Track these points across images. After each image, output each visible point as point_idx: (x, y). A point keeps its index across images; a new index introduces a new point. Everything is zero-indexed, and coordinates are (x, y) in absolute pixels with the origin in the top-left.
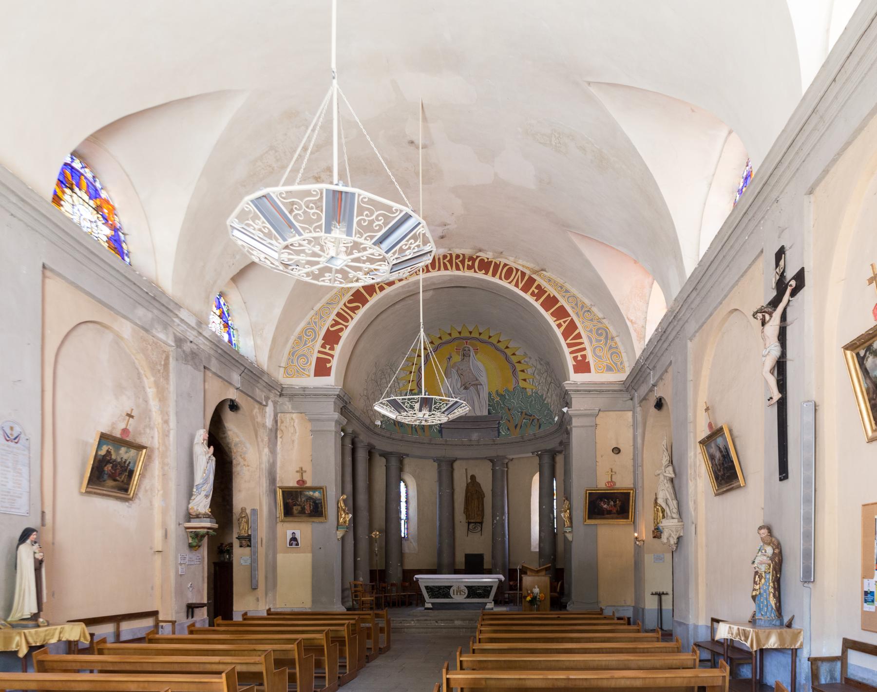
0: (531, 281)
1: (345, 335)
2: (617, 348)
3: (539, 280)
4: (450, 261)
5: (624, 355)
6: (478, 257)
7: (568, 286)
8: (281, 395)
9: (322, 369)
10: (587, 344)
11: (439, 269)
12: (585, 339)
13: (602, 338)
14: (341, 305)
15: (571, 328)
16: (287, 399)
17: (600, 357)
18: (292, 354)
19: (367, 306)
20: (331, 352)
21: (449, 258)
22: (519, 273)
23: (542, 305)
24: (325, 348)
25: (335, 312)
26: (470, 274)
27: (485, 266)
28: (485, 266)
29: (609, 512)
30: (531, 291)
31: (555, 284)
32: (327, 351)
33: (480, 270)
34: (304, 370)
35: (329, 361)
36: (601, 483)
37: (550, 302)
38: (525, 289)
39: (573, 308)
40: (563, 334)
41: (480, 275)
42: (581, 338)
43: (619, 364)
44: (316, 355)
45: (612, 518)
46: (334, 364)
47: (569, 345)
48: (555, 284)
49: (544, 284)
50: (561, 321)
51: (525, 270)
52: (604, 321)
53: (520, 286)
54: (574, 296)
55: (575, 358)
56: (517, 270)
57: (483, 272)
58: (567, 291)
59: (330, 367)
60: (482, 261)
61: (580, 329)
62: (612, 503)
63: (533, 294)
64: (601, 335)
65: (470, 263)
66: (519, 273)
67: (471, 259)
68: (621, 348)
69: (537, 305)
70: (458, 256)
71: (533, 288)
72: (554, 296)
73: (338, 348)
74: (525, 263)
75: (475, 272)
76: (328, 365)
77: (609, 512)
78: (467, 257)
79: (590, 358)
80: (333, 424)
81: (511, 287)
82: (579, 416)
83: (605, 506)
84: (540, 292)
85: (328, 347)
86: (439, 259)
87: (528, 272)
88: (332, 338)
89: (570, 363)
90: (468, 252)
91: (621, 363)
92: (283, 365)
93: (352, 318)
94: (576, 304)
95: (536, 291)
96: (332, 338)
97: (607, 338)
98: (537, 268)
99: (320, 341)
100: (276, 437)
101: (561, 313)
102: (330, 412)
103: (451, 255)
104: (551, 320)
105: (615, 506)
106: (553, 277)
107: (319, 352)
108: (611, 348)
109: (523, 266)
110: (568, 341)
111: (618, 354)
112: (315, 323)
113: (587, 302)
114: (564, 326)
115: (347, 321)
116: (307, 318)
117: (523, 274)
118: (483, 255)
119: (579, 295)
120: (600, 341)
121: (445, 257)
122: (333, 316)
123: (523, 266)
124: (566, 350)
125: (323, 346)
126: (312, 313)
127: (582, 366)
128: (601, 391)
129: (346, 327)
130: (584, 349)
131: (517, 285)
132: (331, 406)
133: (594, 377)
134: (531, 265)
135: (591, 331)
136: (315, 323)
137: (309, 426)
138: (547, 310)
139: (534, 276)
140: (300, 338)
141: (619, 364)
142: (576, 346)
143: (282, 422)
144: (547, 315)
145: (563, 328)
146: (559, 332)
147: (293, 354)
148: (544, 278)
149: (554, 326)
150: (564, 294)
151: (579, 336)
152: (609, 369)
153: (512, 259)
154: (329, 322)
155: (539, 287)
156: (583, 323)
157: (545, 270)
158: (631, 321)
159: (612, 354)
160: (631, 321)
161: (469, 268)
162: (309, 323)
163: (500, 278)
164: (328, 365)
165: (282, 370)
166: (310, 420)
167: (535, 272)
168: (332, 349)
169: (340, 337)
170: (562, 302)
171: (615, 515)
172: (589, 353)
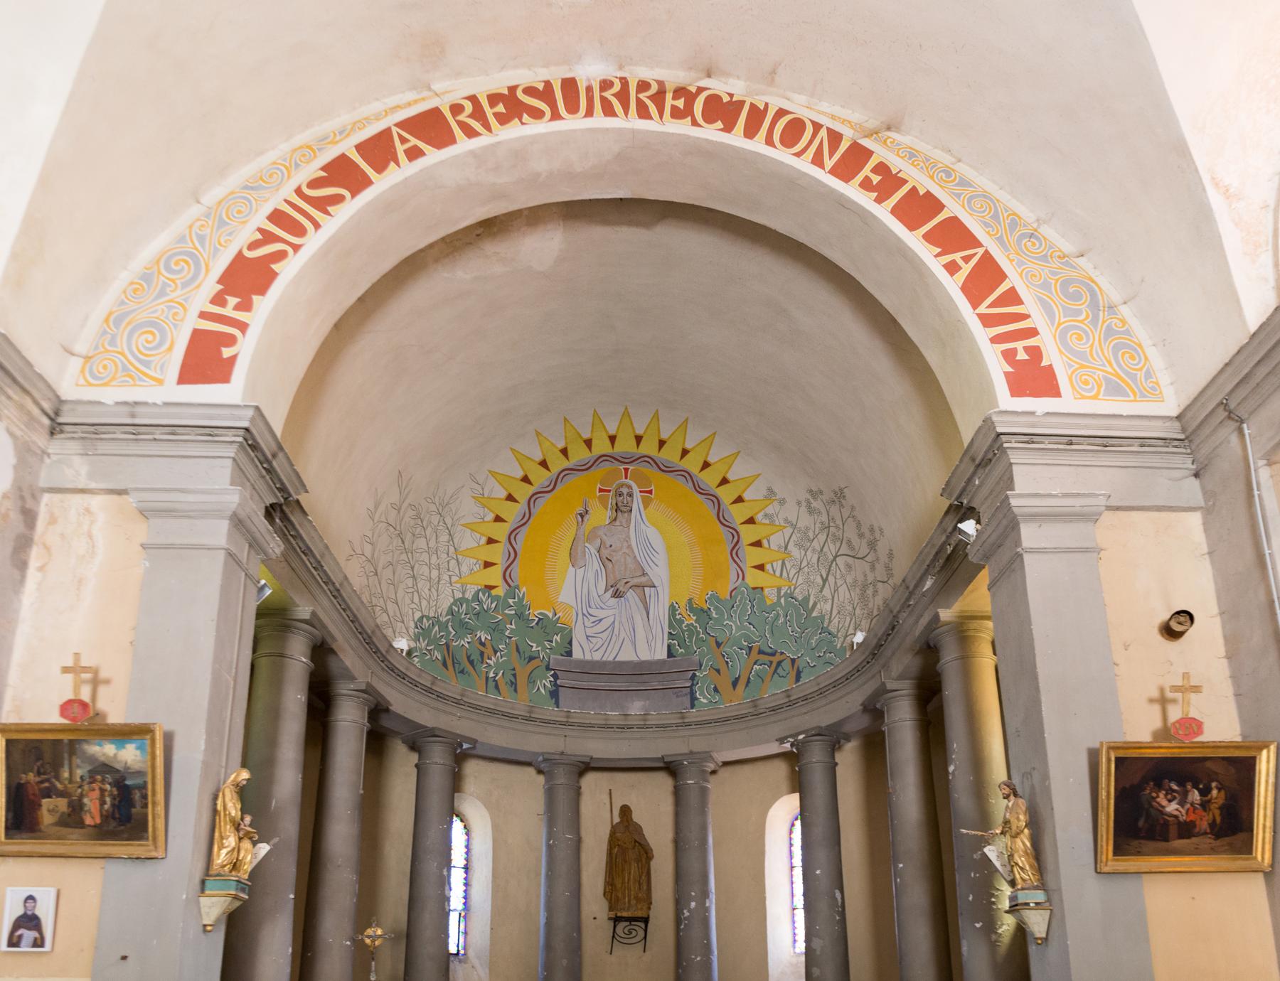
0: (858, 155)
1: (287, 271)
2: (1127, 332)
3: (881, 153)
4: (623, 96)
5: (1151, 352)
6: (701, 90)
7: (964, 169)
8: (55, 429)
9: (206, 360)
10: (1038, 319)
11: (589, 113)
12: (1030, 304)
13: (1085, 312)
14: (288, 191)
15: (985, 278)
16: (74, 446)
17: (1080, 355)
18: (115, 319)
19: (367, 195)
20: (241, 316)
21: (617, 87)
22: (823, 133)
23: (895, 211)
24: (223, 304)
25: (268, 209)
26: (682, 128)
27: (722, 111)
28: (722, 111)
29: (1186, 830)
30: (860, 177)
31: (930, 166)
32: (228, 311)
33: (709, 119)
34: (147, 364)
35: (231, 340)
36: (1139, 728)
37: (918, 208)
38: (845, 170)
39: (986, 225)
40: (965, 289)
41: (712, 133)
42: (1019, 301)
43: (1141, 375)
44: (191, 322)
45: (1196, 852)
46: (245, 350)
47: (987, 321)
48: (930, 166)
49: (897, 164)
50: (957, 257)
51: (837, 127)
52: (1081, 262)
53: (829, 164)
54: (986, 196)
55: (1009, 356)
56: (817, 127)
57: (719, 124)
58: (964, 183)
59: (233, 359)
60: (713, 100)
61: (1014, 279)
62: (1195, 796)
63: (866, 185)
64: (1076, 297)
65: (680, 103)
66: (823, 133)
67: (680, 92)
68: (1141, 333)
69: (883, 213)
70: (643, 86)
71: (866, 171)
72: (928, 194)
73: (264, 305)
74: (838, 110)
75: (695, 123)
76: (227, 352)
77: (1186, 830)
78: (670, 88)
79: (1053, 356)
80: (224, 526)
81: (804, 165)
82: (1034, 517)
83: (1172, 808)
84: (887, 182)
85: (232, 301)
86: (589, 89)
87: (848, 135)
88: (247, 278)
89: (997, 369)
90: (674, 76)
91: (1148, 375)
92: (81, 347)
93: (317, 226)
94: (996, 217)
95: (876, 179)
96: (247, 278)
97: (1094, 305)
98: (872, 124)
99: (210, 286)
100: (22, 566)
101: (952, 236)
102: (218, 484)
103: (624, 82)
104: (926, 253)
105: (1205, 805)
106: (920, 145)
107: (203, 315)
108: (1109, 332)
109: (833, 117)
110: (983, 309)
111: (1135, 349)
112: (201, 239)
113: (1027, 214)
114: (966, 269)
115: (300, 231)
116: (179, 225)
117: (835, 138)
118: (718, 86)
119: (1003, 196)
120: (1079, 312)
121: (605, 85)
122: (260, 219)
123: (833, 117)
124: (981, 335)
125: (218, 300)
126: (195, 211)
127: (1033, 377)
128: (1106, 443)
129: (296, 248)
130: (1033, 332)
131: (818, 161)
132: (224, 470)
133: (1073, 402)
134: (856, 117)
135: (1046, 286)
136: (201, 239)
137: (142, 531)
138: (912, 227)
139: (866, 143)
140: (147, 278)
141: (1141, 375)
142: (1007, 317)
143: (53, 521)
144: (914, 240)
145: (962, 275)
146: (952, 285)
147: (118, 322)
148: (896, 148)
149: (936, 266)
150: (958, 190)
151: (1012, 297)
152: (1115, 389)
153: (802, 99)
154: (248, 234)
155: (882, 168)
156: (1020, 264)
157: (898, 130)
158: (1226, 192)
159: (1117, 348)
160: (1226, 192)
161: (677, 114)
162: (182, 239)
163: (769, 142)
164: (227, 352)
165: (75, 364)
166: (145, 513)
167: (871, 134)
168: (245, 306)
169: (274, 275)
170: (953, 208)
171: (1208, 841)
172: (1048, 342)
